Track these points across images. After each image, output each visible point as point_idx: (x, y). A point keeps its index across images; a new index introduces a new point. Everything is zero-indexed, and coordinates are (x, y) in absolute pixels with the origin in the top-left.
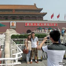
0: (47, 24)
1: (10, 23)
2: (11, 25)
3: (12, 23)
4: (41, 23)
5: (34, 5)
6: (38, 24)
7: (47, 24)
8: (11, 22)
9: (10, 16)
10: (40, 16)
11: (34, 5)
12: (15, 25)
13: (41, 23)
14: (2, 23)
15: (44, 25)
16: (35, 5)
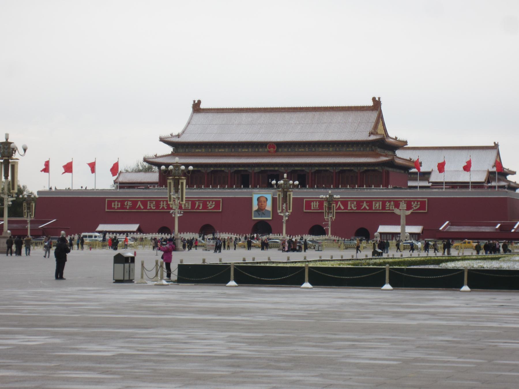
0: (384, 203)
1: (251, 199)
2: (255, 207)
3: (258, 199)
4: (363, 202)
5: (371, 103)
6: (352, 202)
7: (384, 207)
8: (255, 197)
9: (257, 169)
10: (372, 168)
11: (371, 103)
12: (269, 207)
13: (363, 202)
14: (223, 198)
15: (371, 208)
16: (377, 104)
